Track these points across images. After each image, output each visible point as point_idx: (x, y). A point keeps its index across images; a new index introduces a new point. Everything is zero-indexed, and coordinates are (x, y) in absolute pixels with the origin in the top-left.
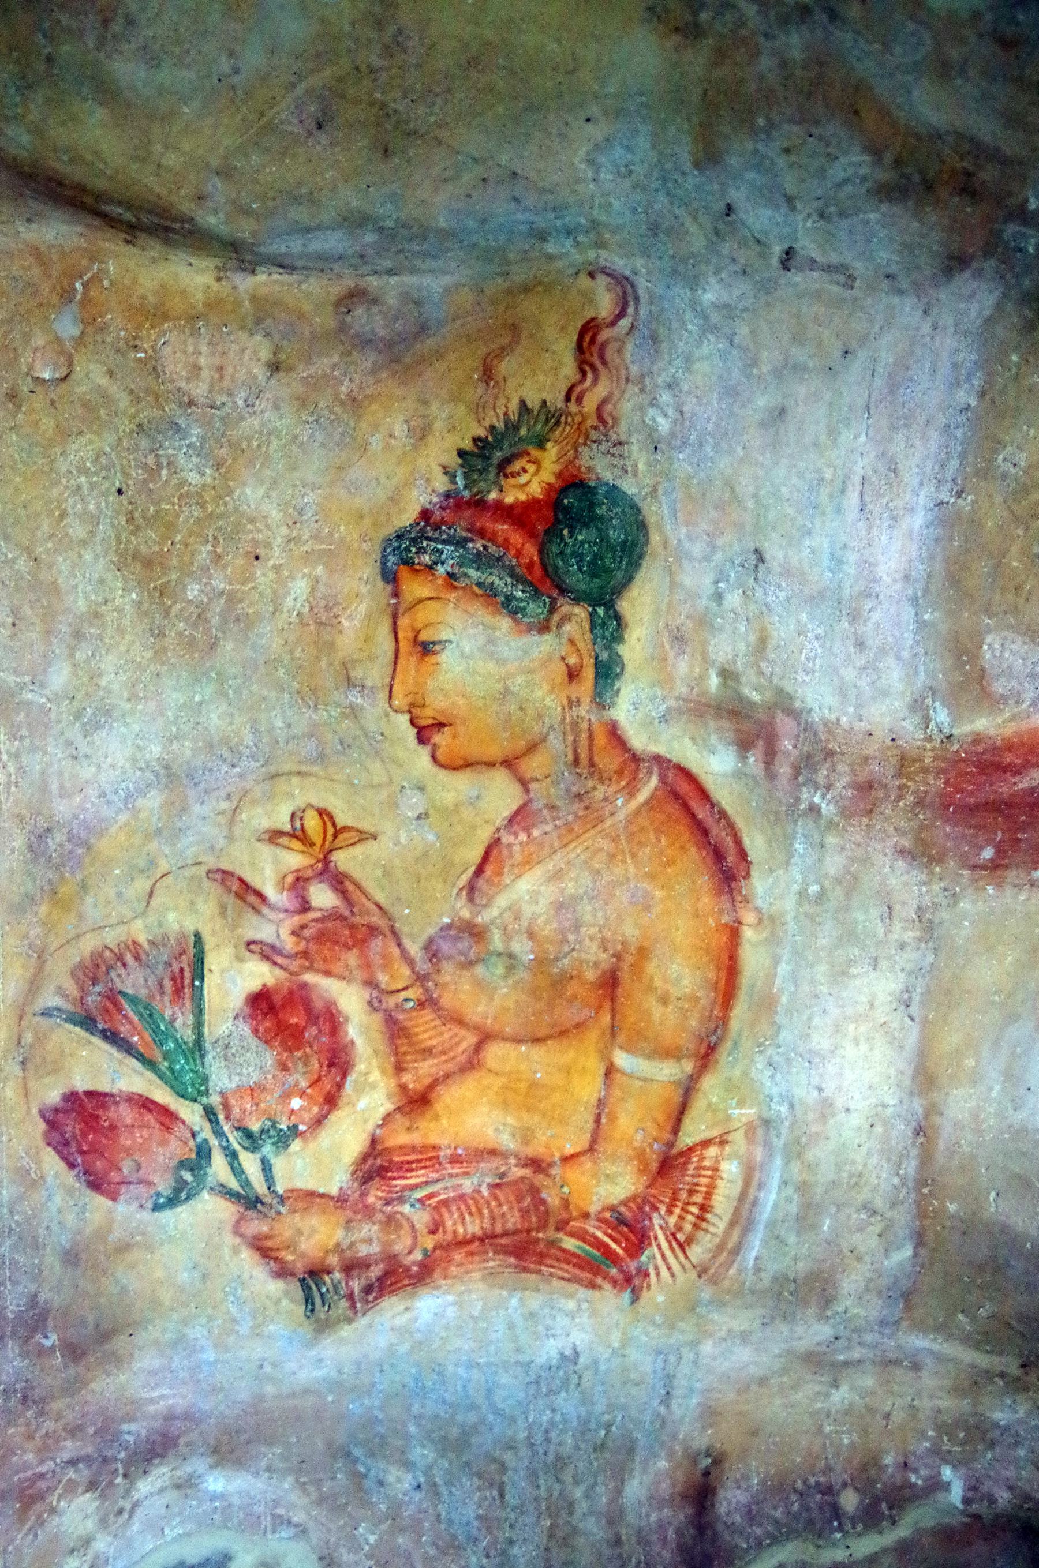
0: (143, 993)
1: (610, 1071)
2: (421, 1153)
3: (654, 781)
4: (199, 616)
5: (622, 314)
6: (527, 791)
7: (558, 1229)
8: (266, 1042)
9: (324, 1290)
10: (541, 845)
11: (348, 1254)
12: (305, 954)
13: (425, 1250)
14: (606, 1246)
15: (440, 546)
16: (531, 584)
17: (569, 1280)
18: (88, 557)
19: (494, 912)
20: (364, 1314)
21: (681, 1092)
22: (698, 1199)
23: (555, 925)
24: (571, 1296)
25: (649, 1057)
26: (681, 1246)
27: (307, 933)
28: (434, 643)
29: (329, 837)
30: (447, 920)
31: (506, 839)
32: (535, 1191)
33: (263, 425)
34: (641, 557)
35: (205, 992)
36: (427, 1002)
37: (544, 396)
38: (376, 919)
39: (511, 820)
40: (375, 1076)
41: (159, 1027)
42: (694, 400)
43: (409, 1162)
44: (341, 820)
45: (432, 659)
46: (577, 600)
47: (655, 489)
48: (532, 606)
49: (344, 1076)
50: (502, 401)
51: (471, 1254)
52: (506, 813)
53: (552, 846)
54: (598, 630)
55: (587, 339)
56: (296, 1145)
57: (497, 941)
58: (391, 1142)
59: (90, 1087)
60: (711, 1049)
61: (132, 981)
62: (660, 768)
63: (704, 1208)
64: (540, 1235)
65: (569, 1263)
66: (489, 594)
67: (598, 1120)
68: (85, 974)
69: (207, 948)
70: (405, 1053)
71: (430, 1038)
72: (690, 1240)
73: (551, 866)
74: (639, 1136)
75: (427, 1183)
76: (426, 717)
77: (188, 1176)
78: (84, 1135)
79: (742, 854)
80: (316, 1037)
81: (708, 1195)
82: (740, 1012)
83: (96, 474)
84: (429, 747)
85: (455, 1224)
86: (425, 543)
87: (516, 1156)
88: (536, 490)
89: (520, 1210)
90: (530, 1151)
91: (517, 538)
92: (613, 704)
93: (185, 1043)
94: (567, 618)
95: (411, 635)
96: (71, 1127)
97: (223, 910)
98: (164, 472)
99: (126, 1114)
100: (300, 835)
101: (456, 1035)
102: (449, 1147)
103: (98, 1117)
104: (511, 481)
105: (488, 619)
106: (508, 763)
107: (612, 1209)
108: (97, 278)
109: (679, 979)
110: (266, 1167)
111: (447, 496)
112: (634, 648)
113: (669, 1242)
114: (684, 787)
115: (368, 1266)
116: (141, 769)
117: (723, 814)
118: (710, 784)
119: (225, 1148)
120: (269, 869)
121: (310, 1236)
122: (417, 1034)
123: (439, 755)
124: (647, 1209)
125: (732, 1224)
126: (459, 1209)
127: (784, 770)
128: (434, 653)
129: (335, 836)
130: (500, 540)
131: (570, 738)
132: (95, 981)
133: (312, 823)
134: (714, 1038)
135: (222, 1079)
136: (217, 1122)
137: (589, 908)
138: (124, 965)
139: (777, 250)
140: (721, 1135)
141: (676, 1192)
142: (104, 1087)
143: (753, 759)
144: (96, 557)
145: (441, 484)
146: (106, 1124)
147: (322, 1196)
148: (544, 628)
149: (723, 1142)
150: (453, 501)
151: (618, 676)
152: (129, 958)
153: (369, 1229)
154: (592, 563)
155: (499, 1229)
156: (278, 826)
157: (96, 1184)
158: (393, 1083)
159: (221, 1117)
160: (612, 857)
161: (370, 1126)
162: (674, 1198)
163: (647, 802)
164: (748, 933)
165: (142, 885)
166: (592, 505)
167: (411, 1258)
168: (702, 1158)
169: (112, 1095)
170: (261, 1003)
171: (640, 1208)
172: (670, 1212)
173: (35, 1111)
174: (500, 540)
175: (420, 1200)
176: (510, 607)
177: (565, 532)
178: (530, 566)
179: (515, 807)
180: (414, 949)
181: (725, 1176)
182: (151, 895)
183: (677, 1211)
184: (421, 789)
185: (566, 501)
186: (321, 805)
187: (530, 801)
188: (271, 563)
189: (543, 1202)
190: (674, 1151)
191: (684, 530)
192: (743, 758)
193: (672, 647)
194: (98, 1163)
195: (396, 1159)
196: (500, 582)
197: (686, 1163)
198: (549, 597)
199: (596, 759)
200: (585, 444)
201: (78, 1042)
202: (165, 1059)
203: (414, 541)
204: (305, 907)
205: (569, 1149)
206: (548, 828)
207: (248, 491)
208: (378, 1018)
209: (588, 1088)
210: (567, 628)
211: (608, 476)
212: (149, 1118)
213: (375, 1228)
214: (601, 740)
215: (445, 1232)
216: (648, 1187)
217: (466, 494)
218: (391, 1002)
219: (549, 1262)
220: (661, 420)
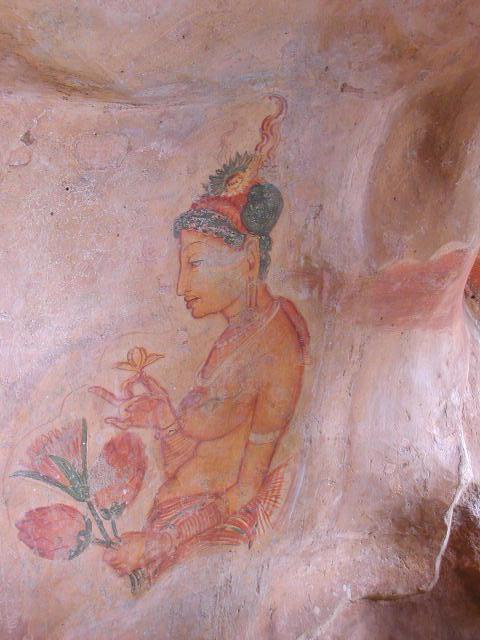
0: (60, 455)
1: (248, 443)
5: (280, 114)
11: (147, 557)
12: (130, 419)
13: (176, 548)
14: (242, 524)
16: (236, 230)
18: (35, 246)
22: (275, 494)
30: (192, 389)
32: (215, 507)
34: (280, 212)
36: (180, 429)
40: (156, 471)
44: (149, 352)
49: (144, 474)
50: (229, 153)
52: (220, 334)
56: (125, 513)
59: (38, 506)
60: (288, 423)
61: (56, 449)
66: (219, 236)
72: (271, 512)
73: (235, 354)
77: (82, 538)
82: (300, 403)
83: (40, 207)
88: (241, 190)
92: (266, 278)
94: (251, 243)
96: (30, 528)
97: (95, 406)
99: (54, 515)
104: (232, 187)
106: (222, 311)
107: (245, 507)
108: (45, 116)
110: (113, 524)
112: (275, 253)
117: (302, 318)
118: (298, 305)
120: (115, 382)
123: (195, 312)
127: (325, 295)
132: (38, 453)
135: (95, 486)
138: (51, 442)
139: (340, 84)
143: (315, 293)
144: (39, 246)
145: (202, 191)
148: (241, 248)
149: (286, 465)
150: (206, 198)
152: (54, 439)
153: (155, 543)
156: (120, 360)
157: (42, 555)
158: (163, 472)
164: (307, 368)
166: (262, 194)
170: (111, 447)
173: (13, 525)
176: (228, 241)
179: (223, 330)
182: (63, 405)
184: (186, 330)
188: (124, 237)
192: (311, 292)
204: (131, 395)
208: (159, 442)
211: (269, 181)
214: (260, 293)
218: (164, 433)
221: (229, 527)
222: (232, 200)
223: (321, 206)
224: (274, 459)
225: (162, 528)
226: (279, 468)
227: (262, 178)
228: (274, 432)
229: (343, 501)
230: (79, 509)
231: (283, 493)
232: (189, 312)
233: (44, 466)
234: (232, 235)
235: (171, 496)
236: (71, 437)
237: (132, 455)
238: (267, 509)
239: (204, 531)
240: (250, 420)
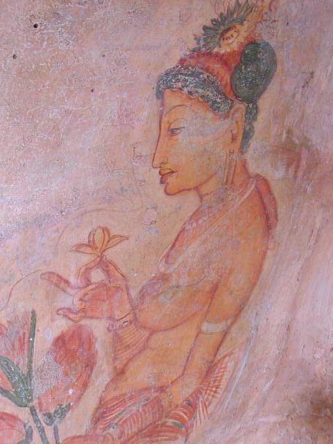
1: (199, 332)
4: (54, 128)
12: (83, 310)
14: (182, 417)
16: (224, 95)
17: (168, 440)
22: (216, 384)
27: (86, 298)
29: (105, 243)
30: (154, 275)
31: (188, 227)
33: (104, 14)
34: (272, 78)
35: (35, 344)
36: (135, 321)
38: (121, 283)
39: (191, 218)
43: (114, 405)
44: (113, 232)
45: (175, 138)
47: (283, 43)
56: (68, 415)
57: (174, 283)
58: (108, 398)
72: (210, 404)
79: (276, 216)
84: (164, 185)
85: (128, 430)
88: (235, 46)
90: (160, 384)
93: (23, 375)
94: (237, 110)
97: (47, 296)
98: (45, 43)
104: (226, 41)
106: (196, 188)
107: (187, 400)
111: (194, 51)
112: (259, 125)
114: (263, 188)
116: (10, 222)
117: (274, 198)
118: (272, 184)
119: (39, 428)
120: (70, 268)
127: (300, 174)
129: (108, 241)
131: (227, 170)
135: (39, 388)
141: (209, 383)
143: (291, 171)
145: (192, 44)
148: (226, 116)
149: (231, 353)
150: (196, 53)
154: (251, 82)
155: (144, 426)
156: (82, 242)
159: (38, 411)
161: (99, 395)
163: (248, 198)
164: (269, 253)
166: (256, 54)
168: (222, 364)
170: (60, 342)
171: (196, 395)
172: (206, 393)
175: (116, 424)
176: (214, 107)
177: (243, 67)
178: (225, 86)
179: (194, 210)
184: (155, 208)
187: (201, 206)
189: (162, 406)
192: (287, 170)
196: (210, 94)
198: (231, 100)
200: (260, 22)
203: (174, 76)
204: (88, 282)
206: (205, 218)
207: (93, 53)
208: (111, 334)
211: (266, 38)
214: (238, 170)
216: (201, 384)
217: (203, 49)
219: (162, 434)
221: (170, 422)
223: (312, 73)
224: (221, 348)
225: (104, 429)
226: (225, 357)
227: (260, 35)
228: (227, 319)
229: (272, 387)
231: (223, 385)
232: (162, 188)
234: (219, 100)
235: (117, 393)
236: (18, 332)
237: (81, 350)
238: (207, 400)
240: (206, 309)
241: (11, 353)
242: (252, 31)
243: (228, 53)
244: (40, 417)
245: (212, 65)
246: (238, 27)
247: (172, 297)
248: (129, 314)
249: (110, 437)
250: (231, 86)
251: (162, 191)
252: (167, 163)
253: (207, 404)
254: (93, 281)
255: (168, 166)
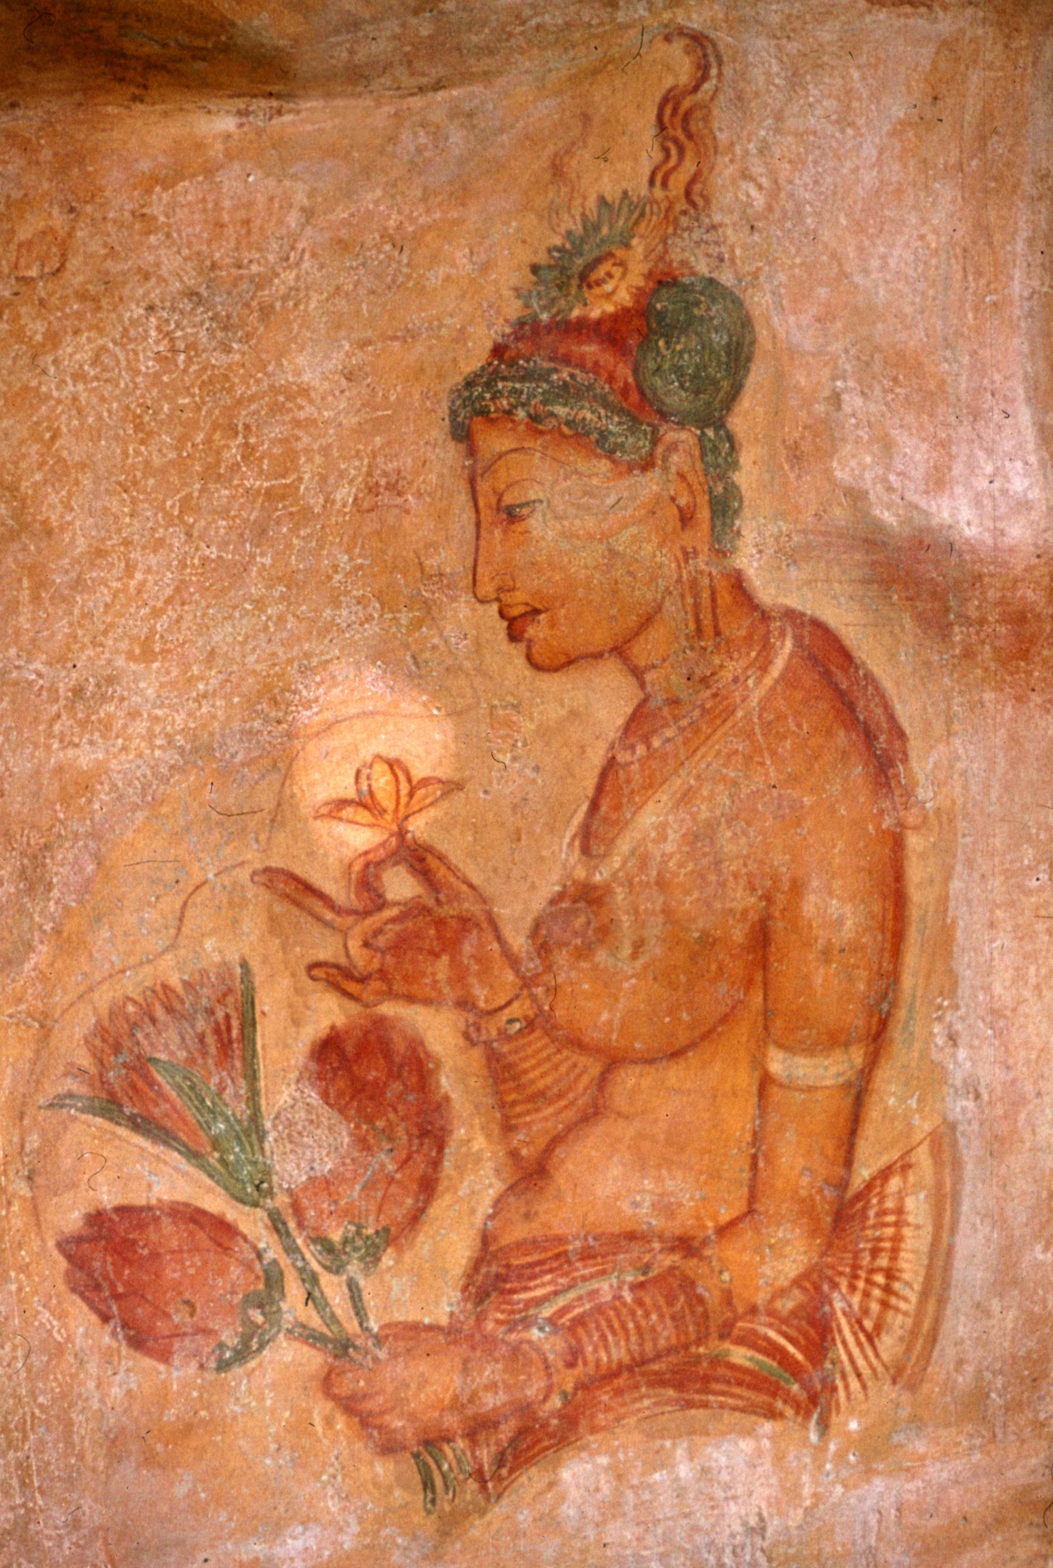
2: (545, 1249)
3: (789, 644)
5: (705, 78)
6: (642, 685)
7: (722, 1337)
8: (341, 1111)
9: (445, 1467)
10: (664, 757)
11: (470, 1412)
12: (382, 974)
13: (564, 1394)
14: (782, 1351)
15: (518, 386)
16: (629, 414)
17: (742, 1410)
19: (616, 862)
20: (499, 1497)
21: (850, 1100)
22: (883, 1262)
23: (690, 866)
24: (749, 1432)
25: (810, 1051)
26: (870, 1338)
28: (521, 506)
29: (404, 800)
31: (623, 757)
32: (688, 1284)
34: (749, 359)
37: (624, 185)
38: (470, 906)
40: (479, 1143)
41: (203, 1101)
42: (788, 166)
43: (531, 1265)
45: (519, 528)
46: (681, 425)
48: (631, 440)
49: (441, 1149)
50: (577, 202)
51: (618, 1392)
52: (620, 721)
53: (676, 756)
54: (709, 458)
55: (668, 111)
56: (388, 1260)
58: (507, 1239)
62: (794, 625)
63: (890, 1274)
64: (701, 1350)
65: (740, 1383)
66: (579, 436)
67: (754, 1166)
68: (104, 1040)
69: (257, 981)
70: (514, 1103)
71: (543, 1075)
72: (878, 1328)
74: (805, 1180)
75: (556, 1293)
76: (518, 601)
78: (119, 1273)
80: (400, 1097)
81: (895, 1252)
84: (522, 647)
85: (596, 1350)
86: (500, 385)
87: (661, 1238)
88: (624, 297)
89: (673, 1318)
90: (675, 1228)
91: (607, 359)
92: (734, 550)
93: (239, 1122)
94: (673, 447)
95: (493, 500)
96: (101, 1263)
100: (367, 802)
101: (575, 1065)
102: (576, 1237)
103: (134, 1242)
104: (597, 291)
105: (582, 466)
106: (620, 651)
109: (840, 921)
110: (354, 1291)
111: (522, 324)
113: (855, 1334)
115: (496, 1425)
119: (301, 1271)
121: (420, 1388)
122: (526, 1072)
124: (826, 1287)
125: (924, 1295)
126: (598, 1327)
128: (522, 519)
129: (411, 795)
130: (589, 365)
131: (690, 600)
132: (117, 1049)
133: (382, 781)
134: (885, 1006)
135: (290, 1170)
136: (288, 1234)
137: (729, 834)
138: (153, 1020)
140: (901, 1157)
141: (856, 1254)
142: (138, 1198)
145: (514, 309)
146: (145, 1252)
147: (431, 1328)
148: (647, 465)
149: (906, 1168)
151: (736, 512)
152: (160, 1013)
153: (490, 1371)
154: (695, 376)
157: (137, 1343)
159: (292, 1225)
160: (748, 760)
161: (479, 1219)
162: (855, 1267)
163: (782, 677)
165: (172, 903)
167: (548, 1406)
168: (882, 1200)
169: (150, 1208)
170: (329, 1050)
171: (817, 1288)
172: (852, 1288)
173: (51, 1243)
174: (589, 365)
175: (550, 1321)
177: (661, 343)
178: (625, 392)
179: (629, 710)
180: (519, 942)
181: (911, 1219)
183: (861, 1284)
185: (659, 306)
186: (392, 755)
189: (701, 1300)
190: (850, 1194)
191: (792, 319)
193: (792, 468)
194: (139, 1311)
195: (515, 1262)
197: (865, 1209)
199: (721, 624)
201: (100, 1138)
202: (215, 1148)
204: (380, 903)
205: (725, 1215)
206: (669, 733)
208: (477, 1053)
209: (739, 1120)
210: (675, 458)
211: (703, 268)
212: (201, 1235)
213: (499, 1366)
214: (725, 598)
215: (585, 1363)
216: (823, 1254)
217: (545, 317)
220: (753, 192)
221: (740, 1355)
222: (604, 328)
227: (684, 263)
230: (244, 1228)
231: (911, 1267)
232: (517, 652)
233: (133, 1086)
239: (658, 1356)
241: (200, 1061)
242: (661, 258)
243: (611, 315)
244: (299, 1241)
245: (574, 348)
246: (620, 253)
247: (634, 956)
248: (517, 996)
249: (534, 1355)
250: (642, 393)
251: (520, 661)
252: (513, 589)
253: (868, 1324)
254: (390, 896)
255: (520, 596)
